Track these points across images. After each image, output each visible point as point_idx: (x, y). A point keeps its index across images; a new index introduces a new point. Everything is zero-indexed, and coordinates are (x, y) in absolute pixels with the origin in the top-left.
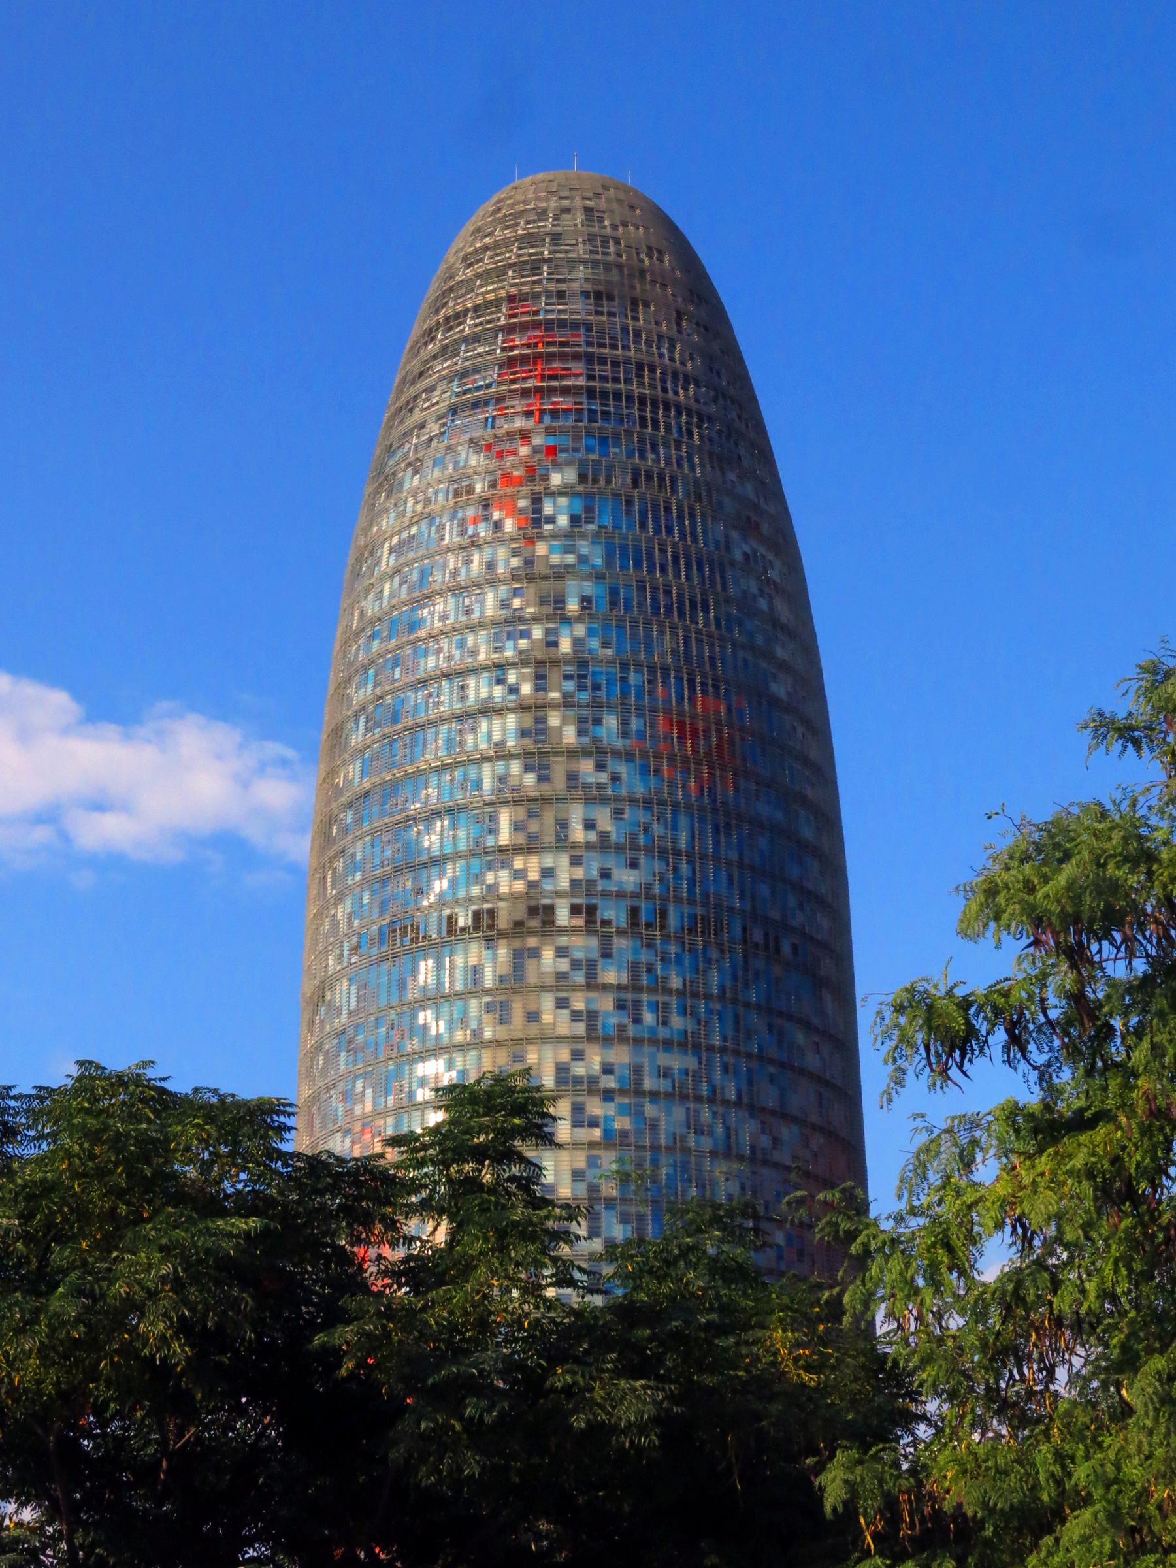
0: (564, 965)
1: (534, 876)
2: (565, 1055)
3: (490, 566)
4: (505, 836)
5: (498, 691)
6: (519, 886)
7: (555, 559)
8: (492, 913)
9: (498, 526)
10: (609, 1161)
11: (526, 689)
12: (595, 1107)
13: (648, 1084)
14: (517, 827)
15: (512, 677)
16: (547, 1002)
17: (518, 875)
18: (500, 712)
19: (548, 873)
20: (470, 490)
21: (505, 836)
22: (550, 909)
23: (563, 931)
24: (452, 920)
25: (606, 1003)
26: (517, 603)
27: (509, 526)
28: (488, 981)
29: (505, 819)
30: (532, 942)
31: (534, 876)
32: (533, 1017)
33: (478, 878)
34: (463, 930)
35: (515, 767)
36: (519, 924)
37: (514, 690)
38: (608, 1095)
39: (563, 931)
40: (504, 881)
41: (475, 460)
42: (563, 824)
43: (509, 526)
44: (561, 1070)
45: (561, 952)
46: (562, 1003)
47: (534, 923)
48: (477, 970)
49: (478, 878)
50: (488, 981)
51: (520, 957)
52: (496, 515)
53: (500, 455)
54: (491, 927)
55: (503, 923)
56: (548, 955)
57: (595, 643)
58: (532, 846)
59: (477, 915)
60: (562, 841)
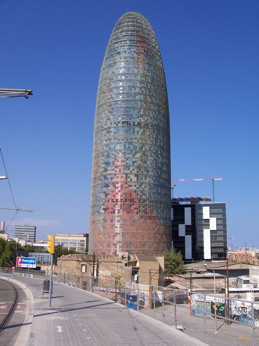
0: (149, 133)
5: (140, 91)
11: (144, 92)
17: (144, 119)
18: (141, 94)
19: (147, 120)
20: (134, 59)
24: (134, 123)
29: (142, 110)
33: (138, 118)
35: (143, 103)
37: (143, 91)
45: (149, 132)
47: (146, 126)
48: (138, 131)
56: (147, 131)
58: (145, 115)
59: (138, 123)
60: (149, 115)
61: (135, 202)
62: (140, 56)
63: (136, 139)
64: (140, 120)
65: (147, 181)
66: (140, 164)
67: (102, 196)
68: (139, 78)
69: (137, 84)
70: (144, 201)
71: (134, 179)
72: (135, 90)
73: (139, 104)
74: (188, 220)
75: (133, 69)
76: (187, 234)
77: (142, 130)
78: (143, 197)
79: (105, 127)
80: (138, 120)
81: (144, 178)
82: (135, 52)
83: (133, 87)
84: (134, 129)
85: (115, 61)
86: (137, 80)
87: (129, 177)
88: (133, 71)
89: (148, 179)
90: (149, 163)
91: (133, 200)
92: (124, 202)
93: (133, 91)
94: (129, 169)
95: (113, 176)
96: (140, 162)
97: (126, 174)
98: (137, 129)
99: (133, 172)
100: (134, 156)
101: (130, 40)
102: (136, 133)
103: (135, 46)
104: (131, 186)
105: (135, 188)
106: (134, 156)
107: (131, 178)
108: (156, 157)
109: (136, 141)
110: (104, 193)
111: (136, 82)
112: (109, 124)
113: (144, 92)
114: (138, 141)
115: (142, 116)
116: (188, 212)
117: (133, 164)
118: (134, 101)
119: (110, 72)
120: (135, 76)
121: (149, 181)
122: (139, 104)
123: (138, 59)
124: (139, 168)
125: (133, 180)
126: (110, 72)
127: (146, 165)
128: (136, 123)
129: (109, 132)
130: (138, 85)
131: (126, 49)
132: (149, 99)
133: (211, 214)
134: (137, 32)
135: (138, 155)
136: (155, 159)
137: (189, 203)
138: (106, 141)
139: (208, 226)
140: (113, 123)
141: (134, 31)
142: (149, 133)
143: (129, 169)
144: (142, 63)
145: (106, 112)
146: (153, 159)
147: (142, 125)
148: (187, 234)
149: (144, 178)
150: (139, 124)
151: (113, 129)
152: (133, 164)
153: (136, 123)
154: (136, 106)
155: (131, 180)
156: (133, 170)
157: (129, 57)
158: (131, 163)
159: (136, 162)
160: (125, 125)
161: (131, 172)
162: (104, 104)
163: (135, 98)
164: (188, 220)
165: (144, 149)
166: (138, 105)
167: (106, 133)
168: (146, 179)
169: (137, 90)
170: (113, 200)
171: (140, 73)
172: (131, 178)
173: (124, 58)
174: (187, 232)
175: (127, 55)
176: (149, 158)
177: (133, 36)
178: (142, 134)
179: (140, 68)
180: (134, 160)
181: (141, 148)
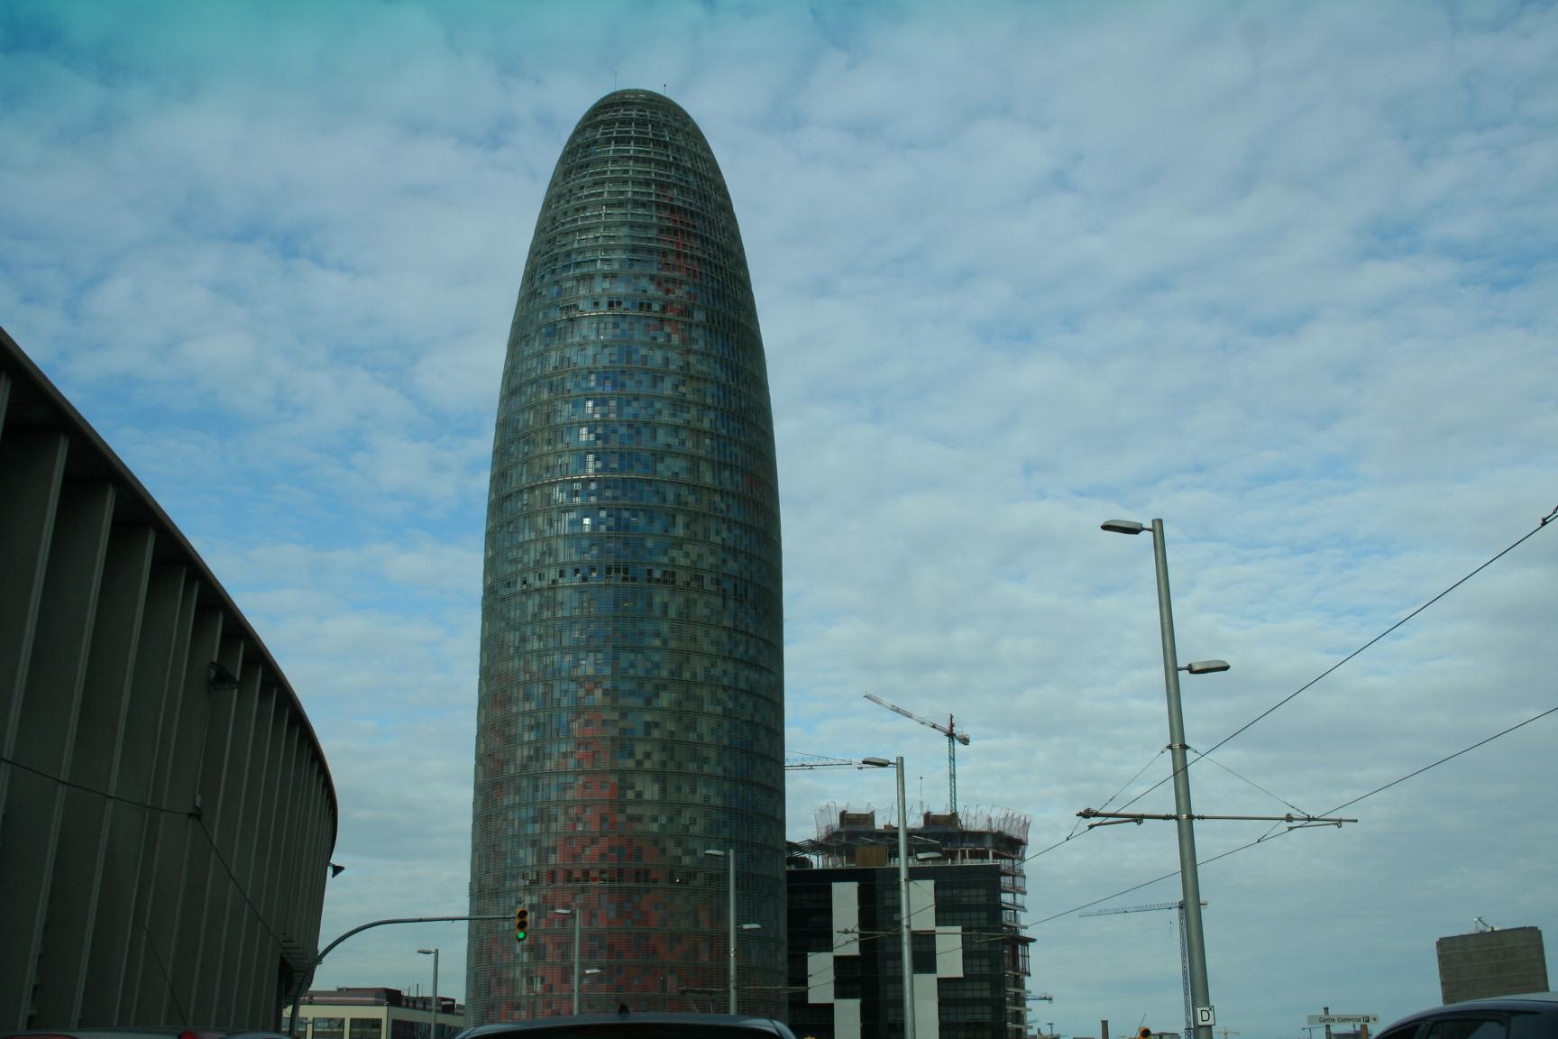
0: (705, 612)
2: (706, 662)
3: (667, 361)
4: (680, 531)
6: (688, 563)
7: (700, 367)
9: (669, 336)
10: (726, 724)
11: (689, 444)
12: (720, 694)
13: (742, 685)
14: (687, 526)
15: (683, 435)
16: (700, 632)
17: (687, 555)
18: (678, 455)
19: (700, 556)
20: (649, 306)
21: (680, 531)
22: (699, 579)
23: (710, 593)
24: (650, 572)
25: (724, 637)
26: (682, 389)
28: (672, 613)
29: (680, 520)
30: (693, 595)
31: (694, 557)
32: (694, 639)
33: (666, 552)
34: (658, 581)
35: (684, 491)
37: (683, 443)
38: (725, 689)
39: (710, 593)
40: (682, 561)
41: (652, 289)
42: (707, 530)
43: (675, 339)
44: (707, 670)
45: (707, 604)
46: (707, 634)
47: (694, 584)
48: (665, 605)
49: (666, 552)
50: (672, 613)
51: (689, 604)
53: (668, 291)
55: (679, 582)
56: (700, 603)
57: (719, 424)
58: (693, 539)
61: (655, 881)
62: (671, 296)
63: (657, 635)
64: (673, 559)
65: (698, 799)
66: (672, 733)
67: (527, 856)
68: (667, 388)
69: (660, 412)
70: (689, 876)
71: (651, 791)
72: (654, 437)
73: (670, 496)
75: (643, 351)
76: (840, 994)
77: (680, 600)
78: (687, 860)
79: (538, 584)
81: (686, 789)
82: (652, 278)
83: (646, 424)
84: (651, 596)
85: (573, 313)
86: (662, 398)
87: (632, 787)
88: (645, 359)
89: (702, 790)
90: (704, 726)
91: (647, 872)
92: (612, 880)
93: (645, 442)
94: (631, 755)
95: (570, 779)
96: (671, 726)
97: (623, 773)
98: (660, 596)
99: (647, 765)
100: (649, 701)
101: (632, 226)
102: (657, 612)
103: (650, 251)
104: (639, 819)
105: (655, 827)
106: (649, 701)
107: (638, 788)
108: (730, 705)
109: (657, 643)
110: (534, 843)
111: (658, 405)
112: (552, 574)
113: (689, 444)
114: (665, 642)
115: (679, 543)
117: (648, 733)
118: (649, 482)
119: (553, 359)
120: (655, 378)
121: (707, 798)
122: (670, 496)
123: (664, 309)
124: (668, 746)
125: (647, 796)
126: (553, 359)
127: (692, 737)
128: (657, 574)
129: (552, 604)
130: (666, 417)
131: (616, 266)
132: (708, 478)
133: (945, 912)
134: (661, 185)
135: (665, 700)
136: (728, 714)
138: (540, 638)
139: (925, 962)
140: (569, 572)
141: (647, 183)
142: (705, 612)
143: (631, 755)
144: (681, 326)
145: (540, 520)
146: (719, 710)
147: (682, 577)
148: (840, 994)
149: (686, 789)
150: (669, 578)
151: (567, 592)
152: (648, 733)
153: (657, 574)
154: (655, 501)
155: (639, 795)
156: (648, 755)
157: (626, 297)
158: (640, 733)
159: (657, 725)
160: (616, 579)
161: (639, 763)
162: (532, 489)
163: (655, 472)
165: (687, 676)
166: (665, 500)
167: (541, 607)
168: (694, 791)
169: (663, 438)
170: (569, 873)
171: (672, 367)
172: (638, 788)
173: (611, 304)
174: (844, 988)
175: (620, 289)
176: (708, 707)
177: (644, 205)
178: (680, 614)
179: (674, 348)
180: (648, 718)
181: (676, 672)
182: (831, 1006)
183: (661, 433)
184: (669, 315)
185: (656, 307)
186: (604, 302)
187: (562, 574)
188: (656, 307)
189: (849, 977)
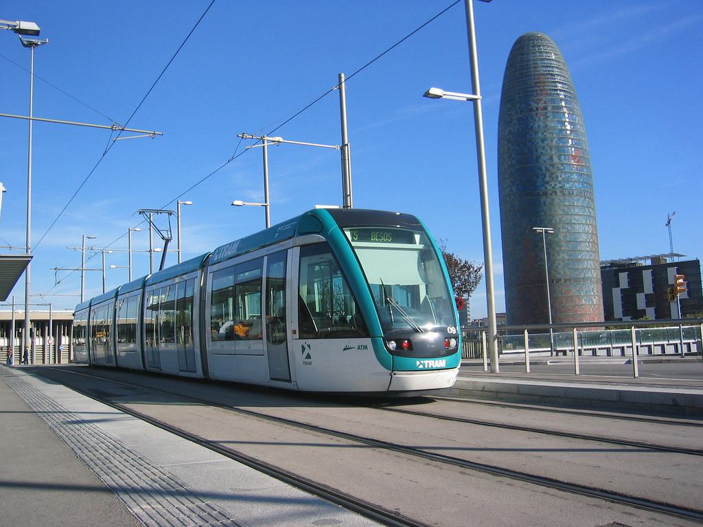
1: (553, 185)
8: (546, 192)
27: (542, 118)
36: (551, 194)
37: (546, 150)
39: (560, 196)
47: (554, 194)
52: (539, 115)
54: (546, 195)
56: (556, 200)
64: (546, 188)
74: (648, 287)
75: (532, 125)
80: (543, 188)
116: (647, 277)
123: (537, 109)
137: (649, 263)
153: (541, 193)
164: (648, 287)
173: (521, 111)
182: (645, 310)
183: (539, 150)
184: (540, 111)
185: (535, 109)
186: (519, 111)
187: (515, 197)
188: (535, 109)
189: (650, 300)
